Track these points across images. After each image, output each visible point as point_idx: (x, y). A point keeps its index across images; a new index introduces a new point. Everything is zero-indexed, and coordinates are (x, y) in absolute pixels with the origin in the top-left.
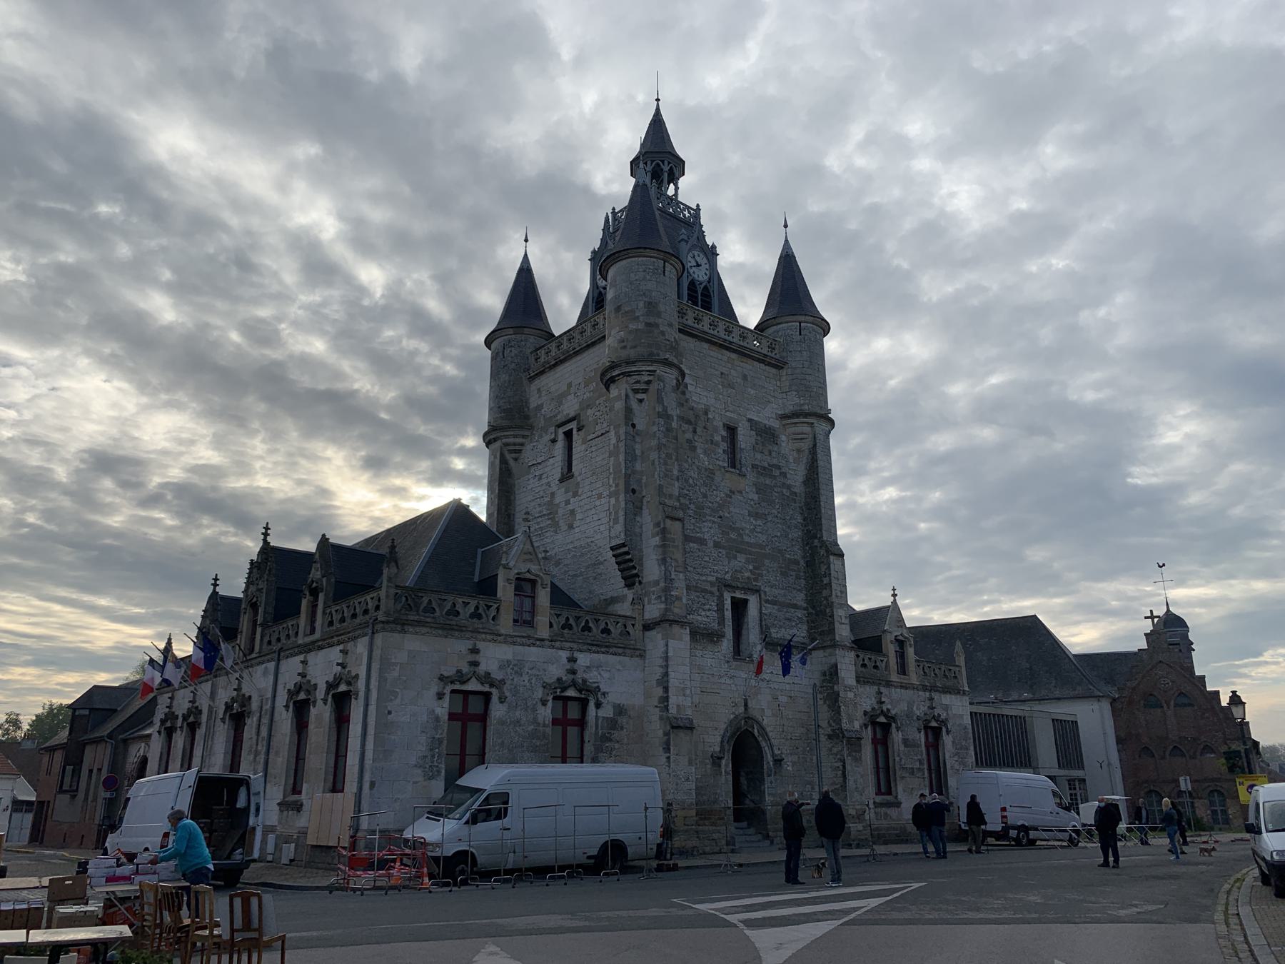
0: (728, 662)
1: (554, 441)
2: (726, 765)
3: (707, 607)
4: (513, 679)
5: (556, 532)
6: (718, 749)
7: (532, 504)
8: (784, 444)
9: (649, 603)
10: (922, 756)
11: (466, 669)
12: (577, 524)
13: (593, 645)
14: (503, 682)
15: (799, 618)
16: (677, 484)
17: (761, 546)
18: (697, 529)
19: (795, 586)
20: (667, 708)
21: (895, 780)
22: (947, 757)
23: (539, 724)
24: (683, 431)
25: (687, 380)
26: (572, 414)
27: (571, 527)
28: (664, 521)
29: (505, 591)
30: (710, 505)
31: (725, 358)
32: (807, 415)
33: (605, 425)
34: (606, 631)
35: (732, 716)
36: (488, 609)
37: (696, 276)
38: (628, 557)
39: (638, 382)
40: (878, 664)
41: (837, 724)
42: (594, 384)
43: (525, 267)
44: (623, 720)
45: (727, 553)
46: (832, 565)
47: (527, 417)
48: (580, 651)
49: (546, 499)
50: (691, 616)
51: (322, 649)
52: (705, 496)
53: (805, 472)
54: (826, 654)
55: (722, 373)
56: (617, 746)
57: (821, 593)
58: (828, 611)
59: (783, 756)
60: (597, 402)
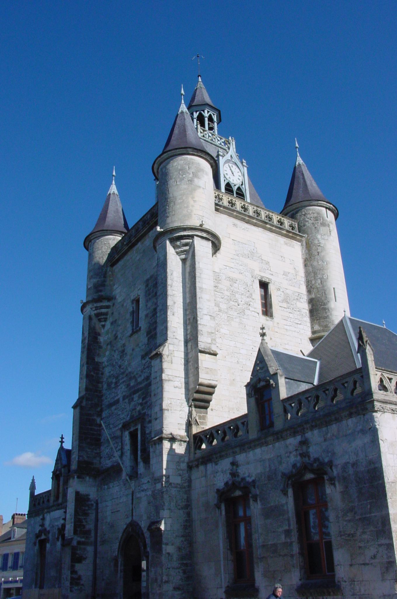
10: (289, 525)
14: (49, 532)
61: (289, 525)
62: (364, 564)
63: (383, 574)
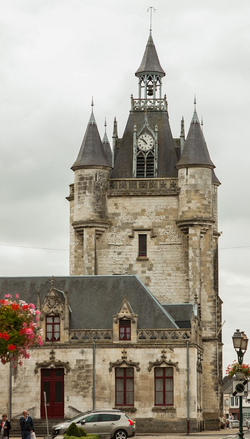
1: (131, 237)
7: (114, 266)
9: (205, 330)
26: (146, 227)
33: (173, 240)
39: (204, 229)
42: (164, 217)
43: (92, 123)
47: (107, 217)
49: (126, 266)
51: (140, 348)
60: (167, 227)
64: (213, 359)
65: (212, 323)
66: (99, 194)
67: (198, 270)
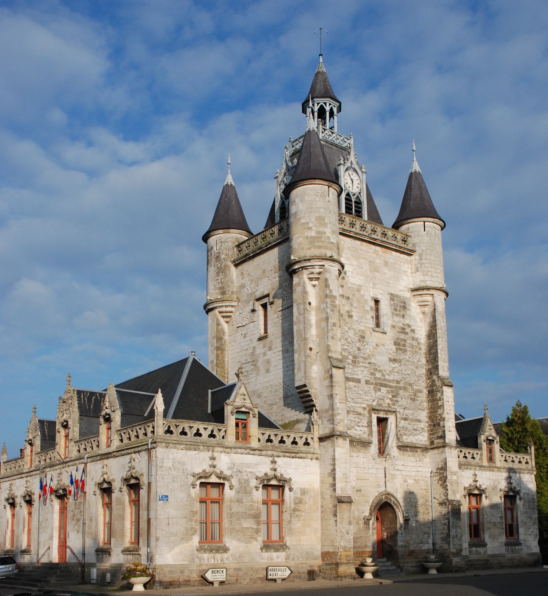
0: (374, 459)
1: (253, 311)
2: (373, 524)
3: (360, 424)
4: (237, 475)
5: (257, 374)
6: (367, 514)
8: (413, 309)
11: (209, 470)
12: (271, 369)
13: (287, 452)
15: (422, 429)
16: (340, 344)
17: (398, 382)
18: (355, 373)
19: (420, 407)
20: (335, 490)
21: (483, 531)
22: (519, 514)
23: (254, 502)
24: (344, 305)
25: (346, 268)
27: (268, 371)
28: (332, 369)
29: (231, 420)
30: (363, 355)
31: (372, 251)
32: (428, 289)
34: (294, 443)
35: (377, 494)
36: (219, 431)
37: (351, 189)
38: (307, 394)
39: (312, 273)
40: (474, 456)
41: (445, 496)
44: (306, 498)
45: (374, 388)
46: (444, 393)
48: (279, 457)
49: (250, 351)
50: (350, 431)
52: (359, 349)
53: (428, 329)
54: (440, 452)
55: (370, 261)
56: (303, 514)
57: (437, 411)
58: (441, 423)
59: (410, 517)
61: (502, 514)
62: (530, 535)
63: (535, 539)
64: (331, 467)
65: (328, 412)
66: (219, 265)
67: (302, 334)
